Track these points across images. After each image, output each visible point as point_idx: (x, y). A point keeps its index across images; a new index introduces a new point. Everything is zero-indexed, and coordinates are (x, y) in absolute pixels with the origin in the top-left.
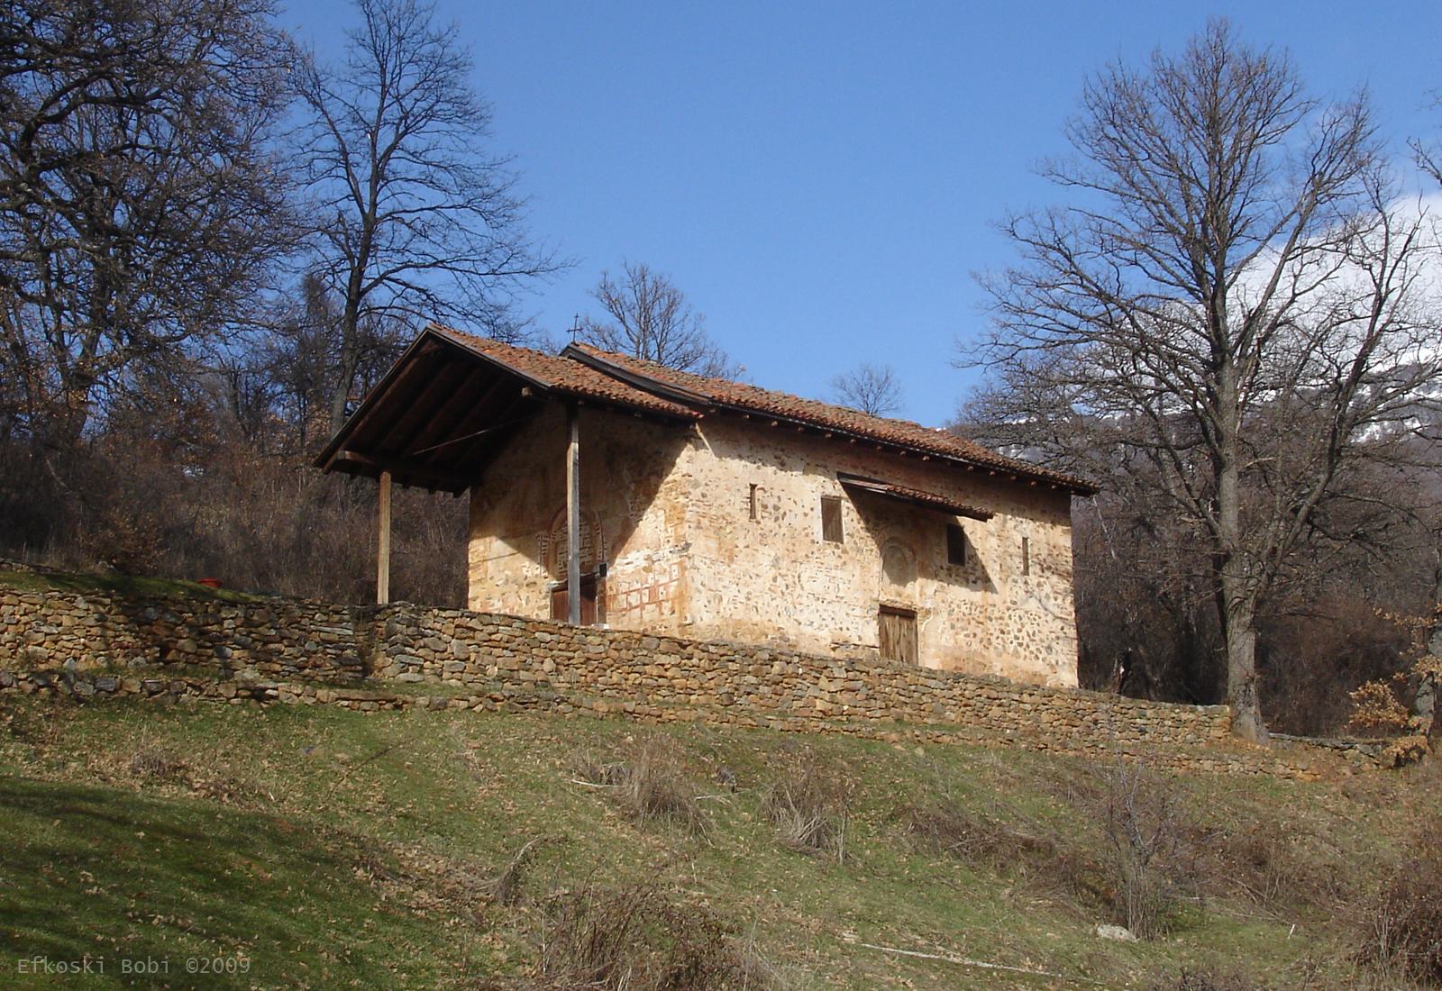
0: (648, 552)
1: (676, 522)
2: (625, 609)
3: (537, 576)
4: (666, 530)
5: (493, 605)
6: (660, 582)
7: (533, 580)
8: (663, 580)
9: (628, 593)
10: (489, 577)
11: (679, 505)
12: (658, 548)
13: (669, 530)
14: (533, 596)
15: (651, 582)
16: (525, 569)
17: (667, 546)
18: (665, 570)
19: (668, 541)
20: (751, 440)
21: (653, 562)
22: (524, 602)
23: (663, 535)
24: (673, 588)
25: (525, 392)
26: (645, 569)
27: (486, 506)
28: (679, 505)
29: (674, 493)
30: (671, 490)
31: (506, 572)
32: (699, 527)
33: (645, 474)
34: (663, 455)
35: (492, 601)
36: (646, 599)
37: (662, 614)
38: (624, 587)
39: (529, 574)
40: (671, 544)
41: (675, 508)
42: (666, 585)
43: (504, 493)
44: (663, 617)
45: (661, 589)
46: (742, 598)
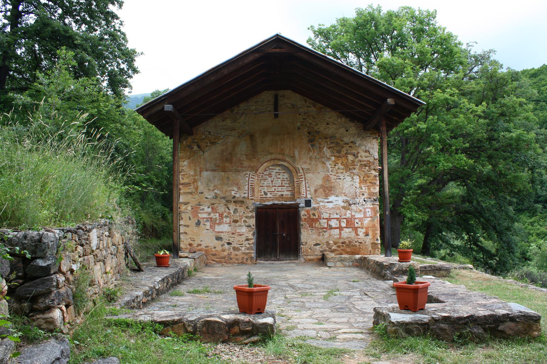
0: (346, 198)
1: (369, 184)
2: (324, 228)
3: (244, 197)
5: (203, 209)
6: (356, 217)
7: (241, 199)
9: (329, 219)
10: (199, 191)
12: (355, 196)
13: (364, 188)
14: (241, 210)
15: (348, 215)
17: (363, 197)
18: (361, 211)
21: (350, 205)
22: (232, 211)
23: (358, 191)
25: (390, 101)
26: (344, 207)
27: (195, 148)
29: (367, 168)
30: (365, 166)
31: (216, 191)
33: (342, 153)
34: (357, 144)
35: (202, 207)
36: (344, 225)
37: (358, 235)
38: (326, 216)
39: (237, 196)
40: (365, 196)
41: (368, 177)
42: (361, 220)
43: (213, 143)
44: (358, 237)
45: (357, 221)
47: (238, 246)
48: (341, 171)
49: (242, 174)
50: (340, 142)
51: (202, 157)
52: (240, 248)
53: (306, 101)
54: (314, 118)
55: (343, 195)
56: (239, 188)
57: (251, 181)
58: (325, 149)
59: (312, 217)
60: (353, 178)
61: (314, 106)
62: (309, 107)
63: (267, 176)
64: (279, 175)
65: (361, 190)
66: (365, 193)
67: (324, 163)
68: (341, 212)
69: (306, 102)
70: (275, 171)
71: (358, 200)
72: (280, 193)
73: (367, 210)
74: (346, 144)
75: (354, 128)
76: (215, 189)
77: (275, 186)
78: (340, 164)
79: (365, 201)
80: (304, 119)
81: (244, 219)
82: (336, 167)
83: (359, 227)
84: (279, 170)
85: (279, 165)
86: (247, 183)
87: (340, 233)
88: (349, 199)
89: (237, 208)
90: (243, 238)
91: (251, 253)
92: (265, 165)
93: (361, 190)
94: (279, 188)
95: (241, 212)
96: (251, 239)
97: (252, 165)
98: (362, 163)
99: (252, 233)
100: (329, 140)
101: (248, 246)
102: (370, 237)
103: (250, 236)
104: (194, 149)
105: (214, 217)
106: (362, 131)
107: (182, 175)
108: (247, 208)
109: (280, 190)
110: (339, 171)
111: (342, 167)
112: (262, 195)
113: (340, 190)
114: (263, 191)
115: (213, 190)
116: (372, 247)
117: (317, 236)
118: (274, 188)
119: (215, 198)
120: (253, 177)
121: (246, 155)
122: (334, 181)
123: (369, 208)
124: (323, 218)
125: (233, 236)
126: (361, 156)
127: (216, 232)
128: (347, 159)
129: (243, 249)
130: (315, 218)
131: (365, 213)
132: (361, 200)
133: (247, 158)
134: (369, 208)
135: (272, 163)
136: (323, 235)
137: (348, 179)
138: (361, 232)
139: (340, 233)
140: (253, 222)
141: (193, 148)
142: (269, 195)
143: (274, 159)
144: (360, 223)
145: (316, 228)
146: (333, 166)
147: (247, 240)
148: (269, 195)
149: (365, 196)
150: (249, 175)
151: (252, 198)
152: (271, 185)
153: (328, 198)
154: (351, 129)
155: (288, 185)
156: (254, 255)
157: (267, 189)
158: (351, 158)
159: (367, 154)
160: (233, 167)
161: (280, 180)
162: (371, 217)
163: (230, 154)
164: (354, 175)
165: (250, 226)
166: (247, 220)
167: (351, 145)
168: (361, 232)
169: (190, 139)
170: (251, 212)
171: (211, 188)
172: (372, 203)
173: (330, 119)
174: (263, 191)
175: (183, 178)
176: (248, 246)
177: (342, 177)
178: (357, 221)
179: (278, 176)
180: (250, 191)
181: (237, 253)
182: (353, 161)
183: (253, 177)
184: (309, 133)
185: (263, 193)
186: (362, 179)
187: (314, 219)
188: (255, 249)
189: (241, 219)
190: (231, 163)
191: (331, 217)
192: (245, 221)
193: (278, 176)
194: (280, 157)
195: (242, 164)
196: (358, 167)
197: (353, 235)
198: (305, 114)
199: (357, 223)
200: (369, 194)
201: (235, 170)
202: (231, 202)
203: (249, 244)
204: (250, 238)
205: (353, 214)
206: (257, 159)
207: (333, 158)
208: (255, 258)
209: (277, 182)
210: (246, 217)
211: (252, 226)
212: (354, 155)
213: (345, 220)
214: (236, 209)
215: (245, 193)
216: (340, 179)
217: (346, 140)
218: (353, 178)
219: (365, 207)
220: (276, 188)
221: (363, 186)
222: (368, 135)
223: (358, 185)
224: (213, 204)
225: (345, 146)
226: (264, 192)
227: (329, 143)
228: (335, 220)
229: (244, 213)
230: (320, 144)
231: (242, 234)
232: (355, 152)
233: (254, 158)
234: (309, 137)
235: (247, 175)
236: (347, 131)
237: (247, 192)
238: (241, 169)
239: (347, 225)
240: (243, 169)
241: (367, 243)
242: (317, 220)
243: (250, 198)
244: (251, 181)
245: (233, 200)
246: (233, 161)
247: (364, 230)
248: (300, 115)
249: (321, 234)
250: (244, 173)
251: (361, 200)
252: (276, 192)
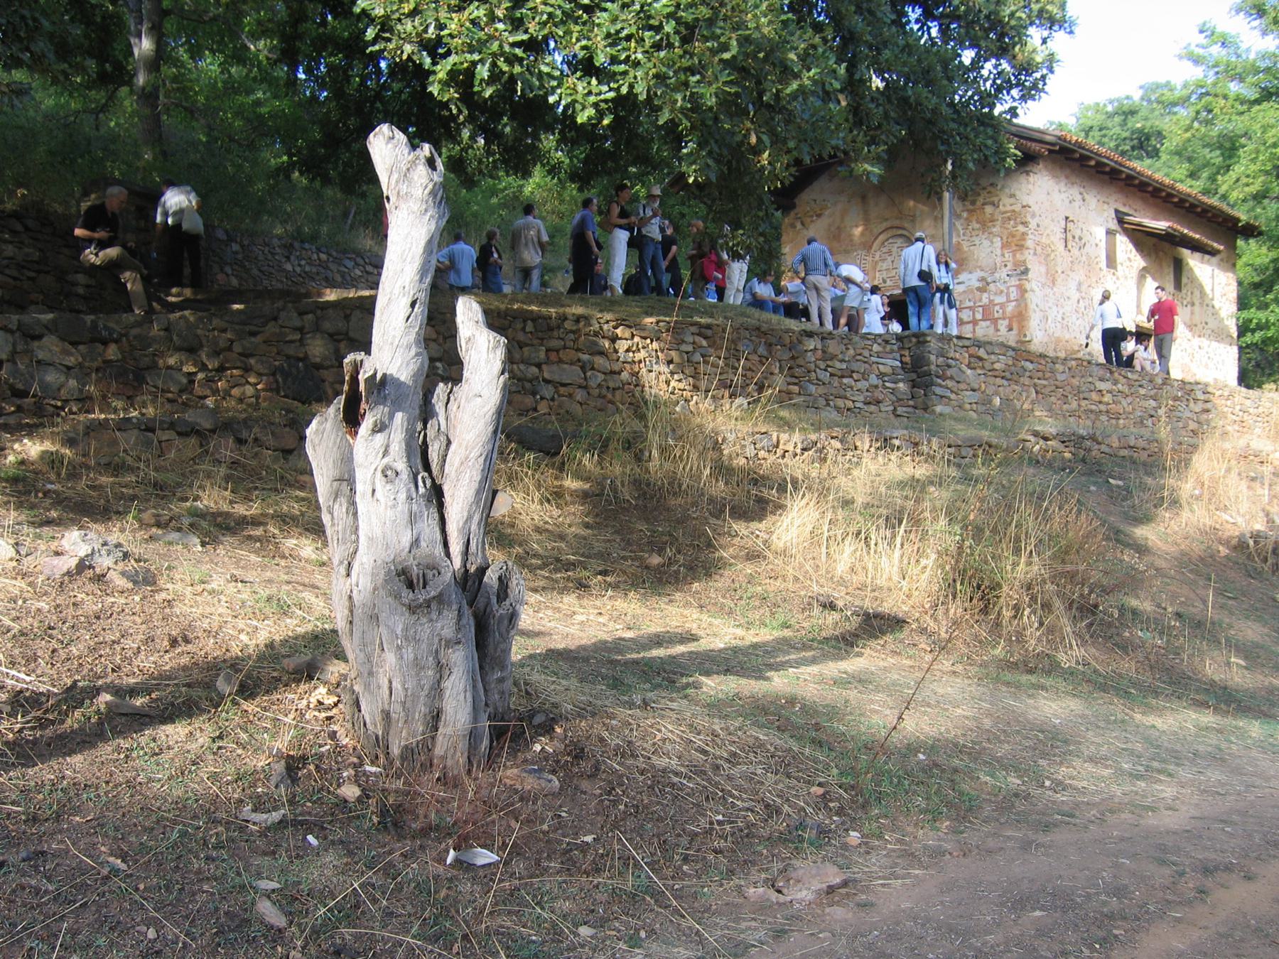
0: (982, 274)
4: (1003, 255)
8: (999, 300)
11: (1018, 234)
12: (994, 270)
15: (985, 300)
17: (1004, 270)
18: (1002, 292)
20: (1067, 177)
21: (988, 284)
23: (999, 260)
24: (1010, 308)
26: (979, 289)
27: (799, 226)
28: (1018, 234)
30: (1009, 219)
32: (1035, 254)
33: (978, 203)
36: (979, 316)
37: (998, 330)
41: (1013, 236)
42: (1002, 306)
43: (819, 216)
45: (997, 308)
46: (1059, 316)
71: (997, 275)
73: (1012, 289)
85: (901, 236)
92: (882, 237)
102: (1014, 332)
111: (978, 226)
131: (1008, 295)
132: (1002, 274)
135: (890, 233)
137: (986, 243)
138: (1003, 325)
142: (889, 283)
143: (887, 229)
148: (889, 283)
159: (1012, 200)
163: (838, 228)
167: (990, 189)
168: (1003, 325)
169: (792, 214)
194: (897, 223)
197: (991, 331)
207: (965, 215)
223: (999, 252)
232: (996, 199)
247: (1006, 322)
251: (1002, 274)
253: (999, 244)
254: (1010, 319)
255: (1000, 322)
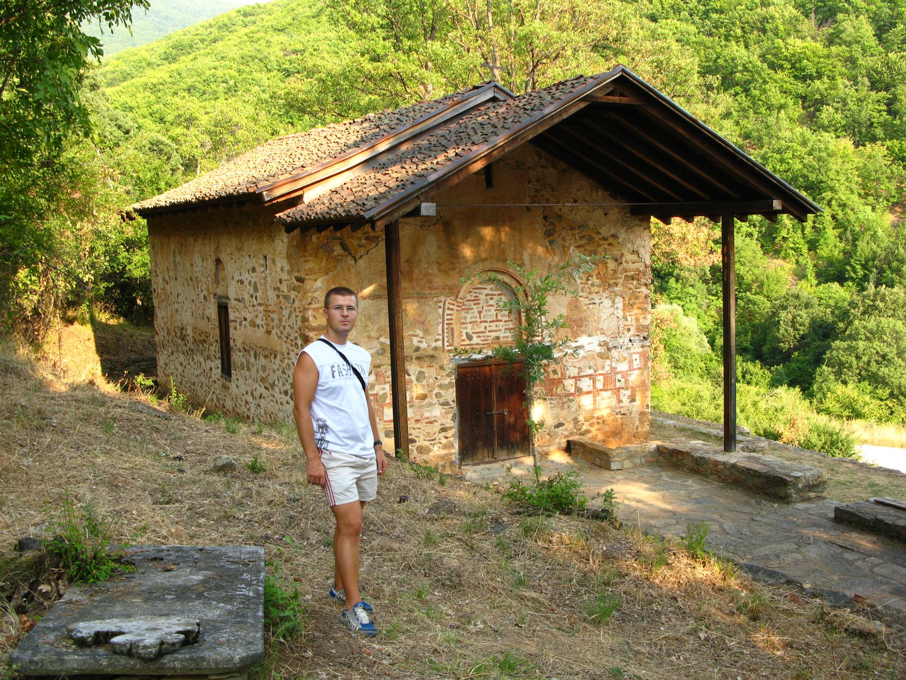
0: (603, 338)
3: (436, 348)
6: (618, 370)
7: (431, 353)
12: (617, 335)
13: (629, 318)
16: (415, 340)
18: (625, 359)
19: (629, 330)
21: (609, 349)
26: (601, 355)
27: (338, 250)
29: (635, 282)
34: (621, 240)
36: (600, 386)
37: (620, 401)
39: (423, 345)
40: (631, 333)
42: (625, 375)
44: (621, 405)
45: (619, 377)
47: (427, 443)
48: (596, 289)
49: (431, 303)
50: (594, 235)
51: (353, 270)
52: (431, 447)
53: (539, 155)
54: (553, 190)
55: (599, 332)
56: (426, 331)
57: (448, 315)
58: (572, 248)
59: (552, 376)
60: (613, 302)
61: (554, 167)
62: (545, 168)
63: (472, 303)
64: (492, 299)
65: (626, 323)
66: (631, 328)
67: (571, 275)
68: (596, 365)
69: (540, 158)
70: (485, 292)
71: (621, 341)
72: (494, 334)
74: (604, 239)
75: (616, 210)
76: (381, 336)
77: (486, 322)
78: (594, 277)
79: (630, 341)
80: (537, 190)
81: (437, 390)
82: (590, 282)
83: (623, 388)
84: (492, 289)
86: (441, 320)
87: (595, 401)
88: (607, 339)
89: (423, 370)
90: (437, 427)
91: (451, 454)
93: (626, 323)
94: (492, 324)
95: (430, 377)
96: (451, 428)
97: (449, 284)
98: (628, 274)
99: (450, 416)
100: (577, 231)
101: (444, 441)
103: (449, 422)
104: (335, 253)
105: (381, 392)
106: (628, 215)
107: (314, 309)
108: (442, 368)
109: (494, 328)
110: (592, 289)
111: (597, 282)
112: (464, 340)
113: (595, 324)
114: (464, 331)
115: (378, 338)
116: (639, 419)
117: (559, 410)
118: (484, 324)
119: (382, 354)
120: (451, 307)
121: (437, 263)
122: (585, 308)
123: (637, 353)
124: (569, 377)
125: (418, 426)
126: (626, 262)
127: (385, 422)
128: (606, 267)
129: (436, 448)
130: (556, 377)
131: (631, 363)
133: (440, 270)
134: (637, 353)
136: (569, 407)
137: (607, 303)
139: (595, 401)
140: (451, 395)
141: (333, 251)
142: (475, 340)
144: (623, 380)
145: (558, 395)
146: (584, 281)
147: (444, 430)
148: (475, 340)
149: (631, 333)
150: (444, 304)
151: (450, 348)
152: (478, 320)
153: (578, 339)
154: (612, 212)
155: (507, 318)
156: (453, 458)
157: (472, 328)
158: (611, 265)
159: (635, 257)
160: (413, 288)
161: (493, 309)
162: (639, 368)
164: (616, 295)
165: (447, 404)
166: (442, 392)
167: (611, 240)
168: (625, 394)
170: (448, 375)
171: (374, 334)
172: (641, 344)
173: (579, 193)
174: (464, 331)
175: (315, 317)
176: (444, 441)
177: (597, 301)
178: (619, 377)
179: (491, 302)
180: (446, 335)
181: (425, 457)
182: (615, 271)
183: (451, 307)
184: (545, 218)
185: (464, 337)
186: (627, 302)
187: (554, 379)
188: (456, 445)
189: (431, 391)
190: (411, 281)
191: (582, 374)
192: (438, 395)
193: (491, 302)
194: (499, 265)
195: (430, 282)
196: (621, 281)
198: (538, 180)
199: (619, 381)
200: (638, 329)
201: (418, 293)
202: (412, 359)
203: (446, 438)
204: (448, 425)
205: (614, 365)
206: (457, 270)
208: (457, 462)
209: (488, 313)
210: (441, 386)
211: (451, 403)
212: (616, 260)
213: (601, 378)
214: (421, 373)
215: (437, 340)
216: (594, 303)
217: (604, 231)
218: (613, 302)
219: (632, 351)
220: (487, 325)
221: (628, 314)
222: (637, 222)
223: (620, 314)
224: (379, 366)
225: (602, 242)
226: (467, 334)
227: (577, 237)
228: (587, 379)
229: (436, 378)
230: (564, 239)
231: (435, 421)
233: (453, 269)
234: (544, 226)
235: (441, 304)
236: (606, 214)
237: (441, 337)
238: (429, 291)
239: (604, 385)
240: (433, 292)
241: (633, 415)
242: (559, 382)
243: (447, 348)
244: (448, 315)
245: (415, 355)
246: (415, 277)
247: (628, 392)
248: (530, 182)
249: (566, 405)
250: (435, 300)
251: (624, 340)
252: (487, 334)
253: (620, 305)
254: (633, 390)
255: (622, 391)
